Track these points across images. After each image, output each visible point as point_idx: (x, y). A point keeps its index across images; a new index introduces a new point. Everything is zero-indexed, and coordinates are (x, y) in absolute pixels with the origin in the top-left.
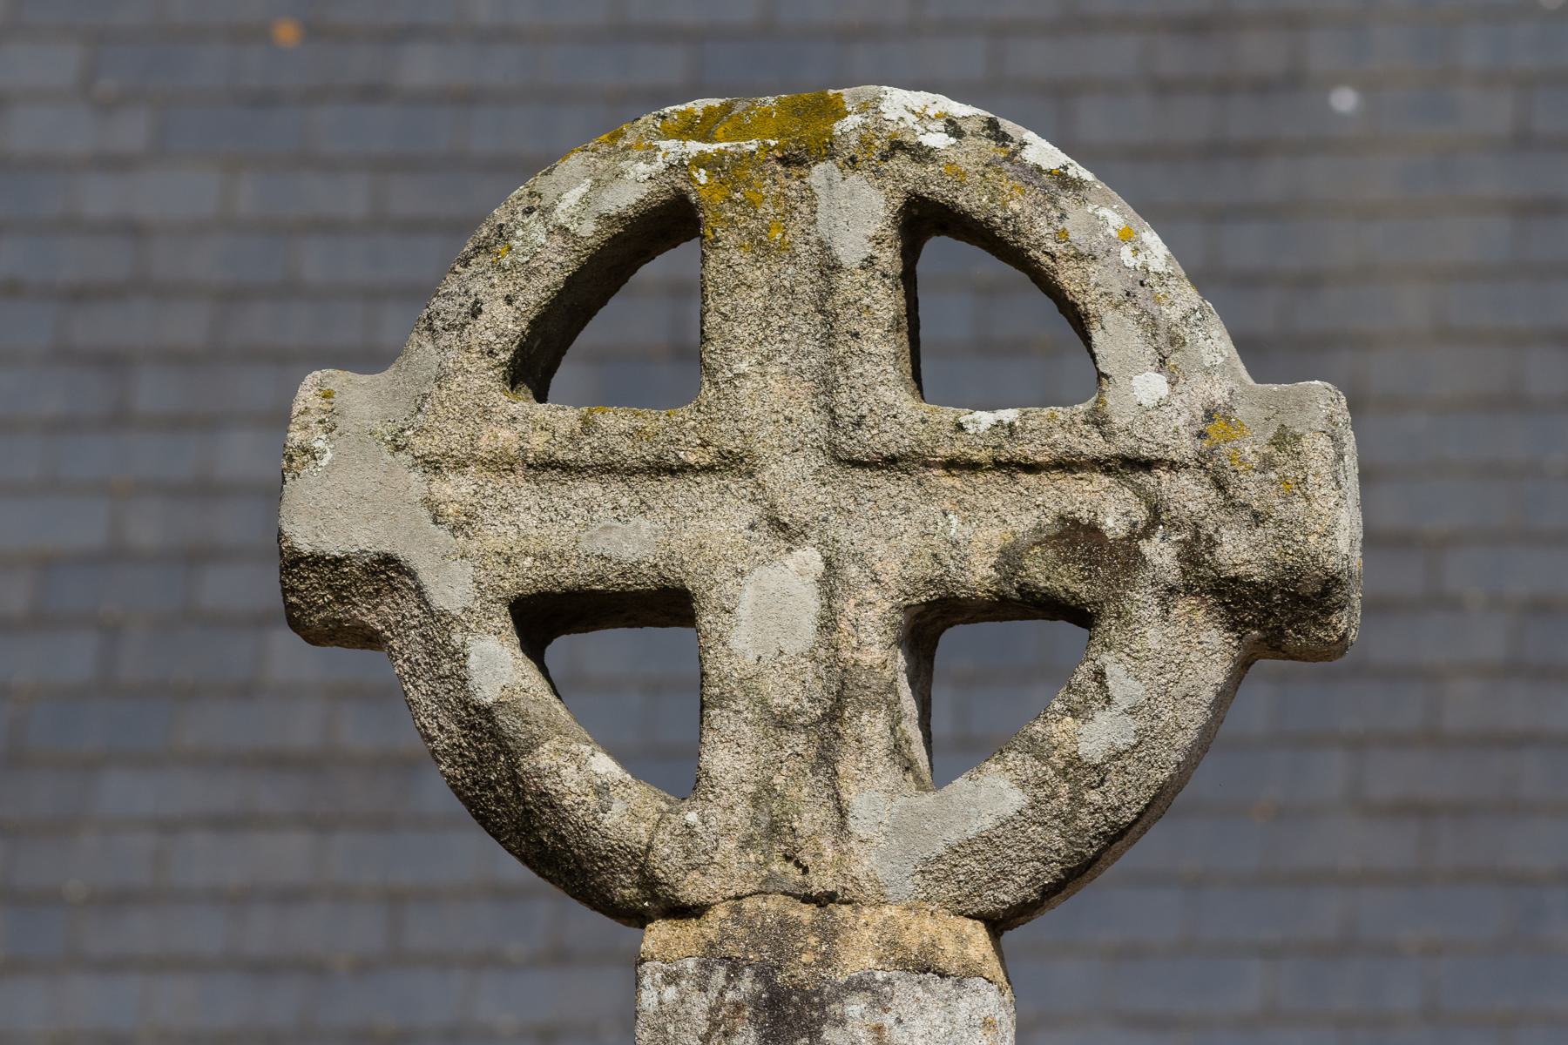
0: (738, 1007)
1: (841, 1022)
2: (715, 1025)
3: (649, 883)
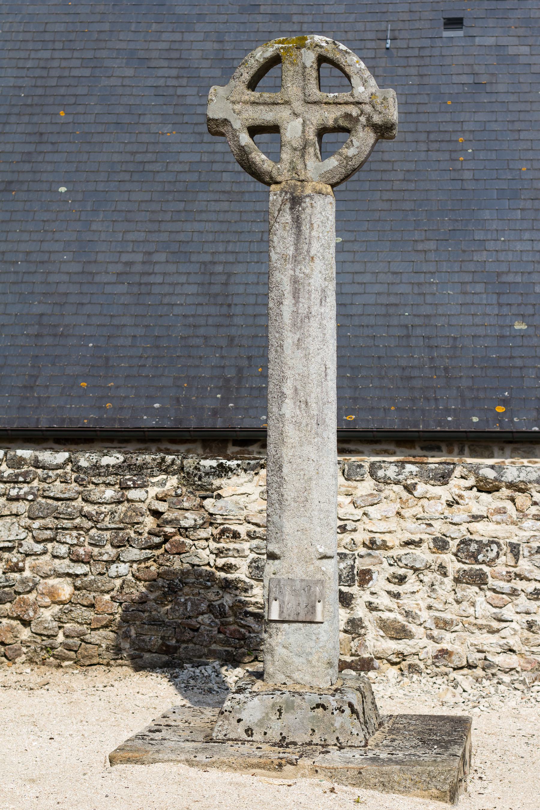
0: (287, 200)
1: (305, 202)
3: (271, 178)
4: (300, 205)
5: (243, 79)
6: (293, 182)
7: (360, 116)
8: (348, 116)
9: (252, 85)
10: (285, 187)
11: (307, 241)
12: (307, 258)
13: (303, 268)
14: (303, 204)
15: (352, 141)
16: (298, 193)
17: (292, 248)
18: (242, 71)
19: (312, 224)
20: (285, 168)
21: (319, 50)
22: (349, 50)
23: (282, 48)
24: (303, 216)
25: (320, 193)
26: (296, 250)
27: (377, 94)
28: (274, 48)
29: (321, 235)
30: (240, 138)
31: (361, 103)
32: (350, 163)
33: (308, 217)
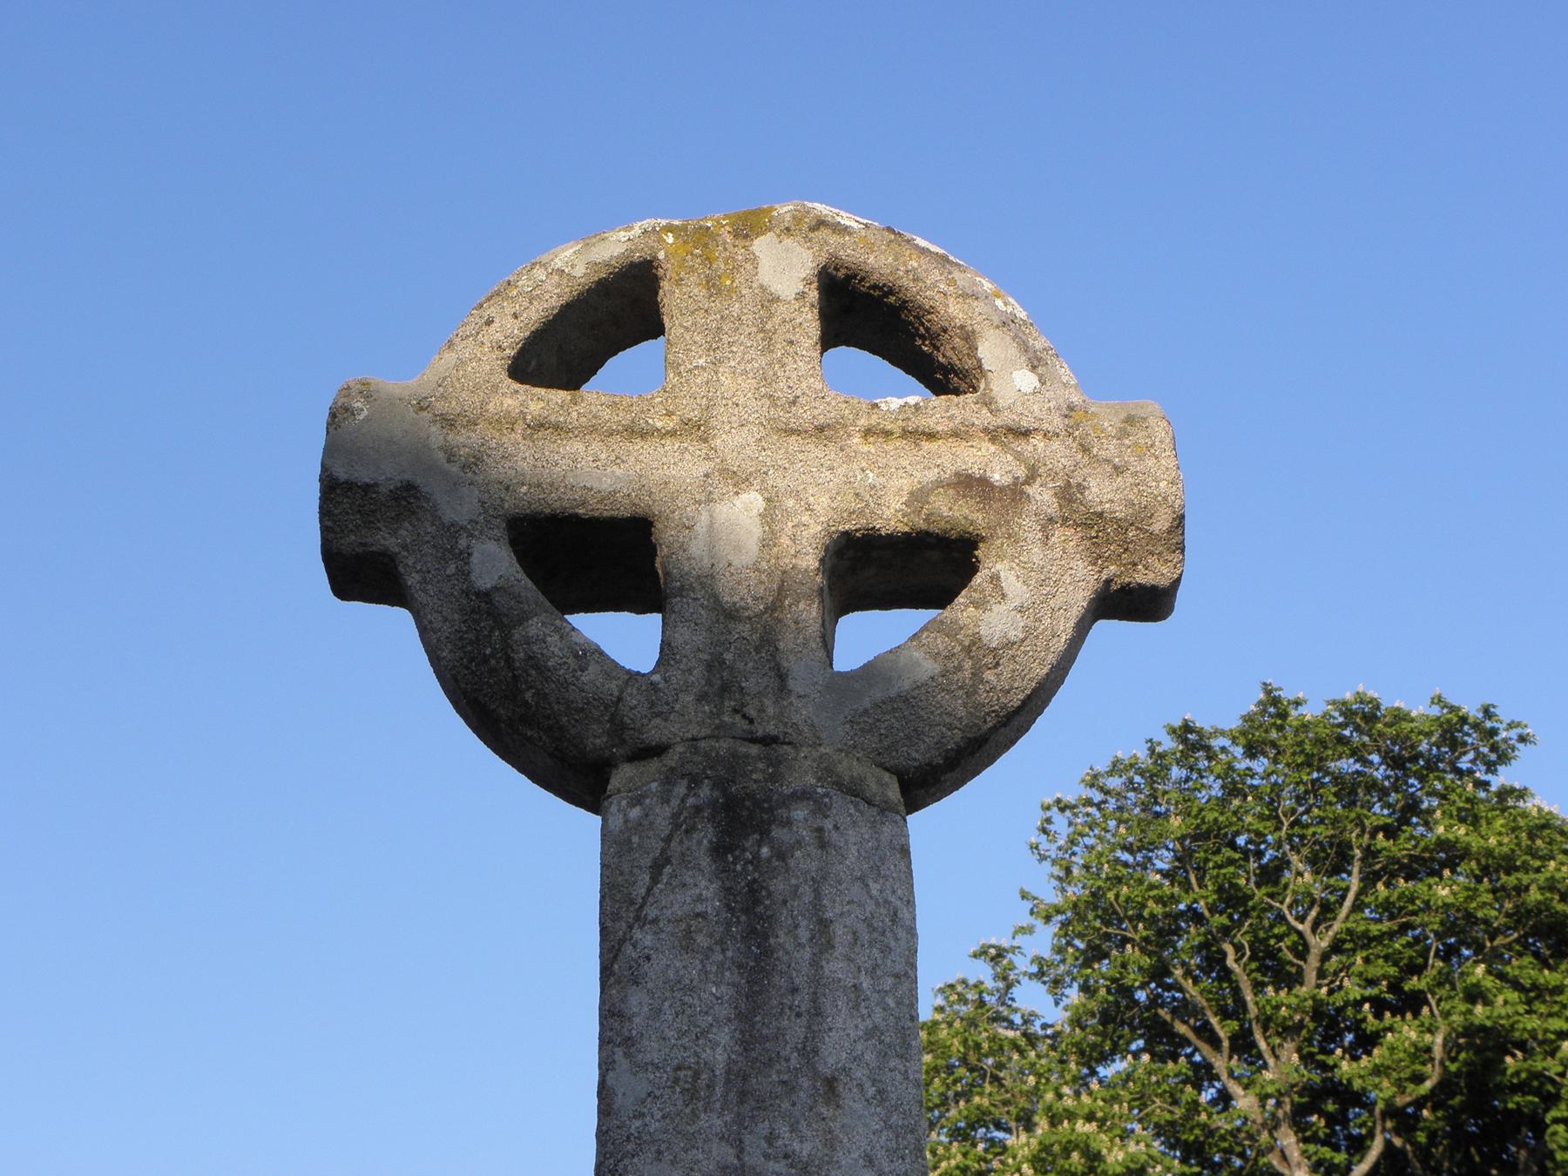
0: (698, 809)
1: (788, 823)
2: (677, 826)
3: (618, 728)
4: (765, 834)
5: (494, 333)
8: (971, 485)
11: (802, 1001)
12: (805, 1083)
13: (784, 1130)
14: (777, 833)
17: (724, 1036)
19: (824, 924)
20: (686, 688)
21: (834, 239)
23: (669, 228)
24: (778, 886)
25: (854, 791)
26: (747, 1042)
29: (866, 983)
30: (476, 558)
31: (1025, 434)
33: (806, 890)
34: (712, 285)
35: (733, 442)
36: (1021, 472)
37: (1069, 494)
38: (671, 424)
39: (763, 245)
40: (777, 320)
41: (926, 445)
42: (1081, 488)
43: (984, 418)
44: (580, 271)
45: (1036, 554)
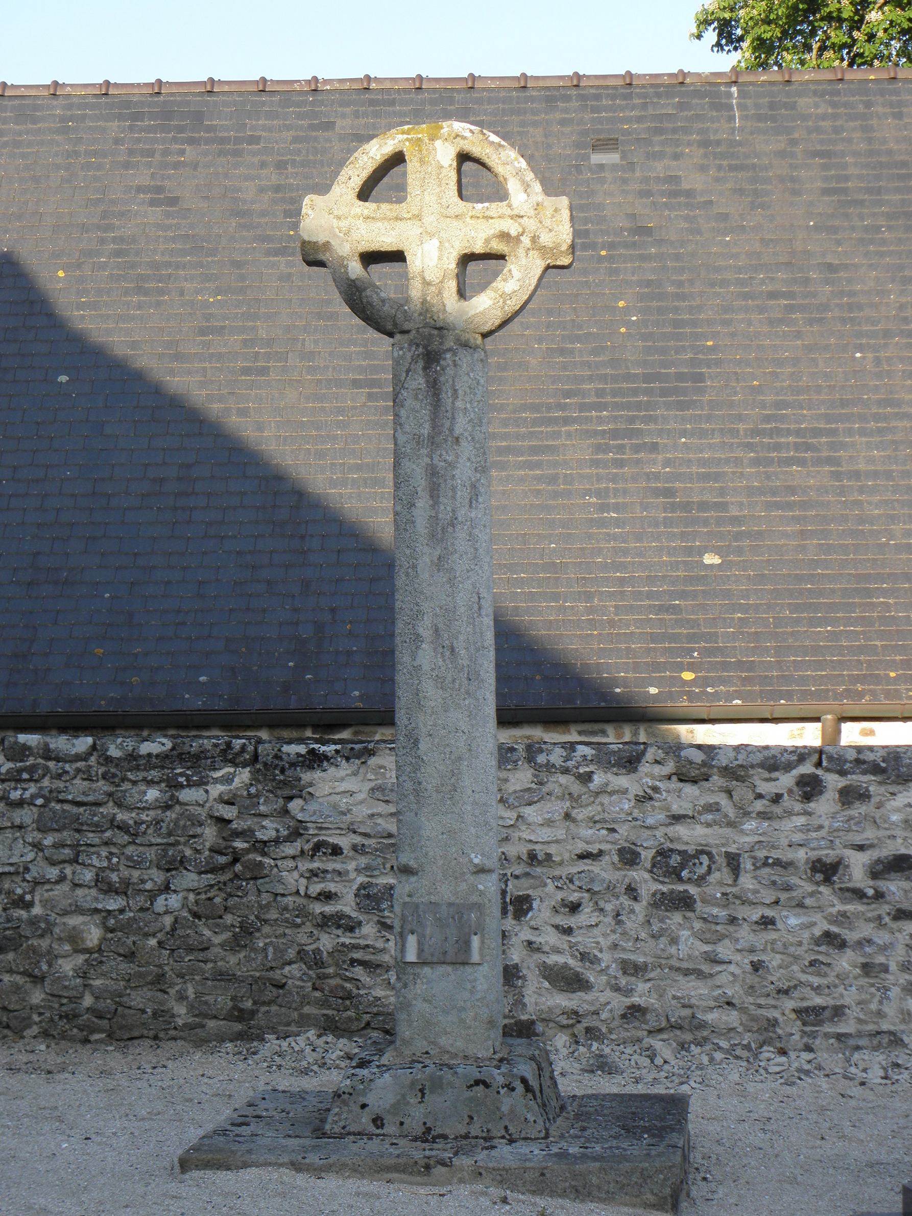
0: (419, 355)
1: (445, 359)
2: (413, 360)
3: (395, 324)
4: (438, 362)
6: (426, 330)
7: (522, 235)
8: (504, 236)
9: (364, 194)
10: (415, 338)
11: (449, 415)
12: (450, 439)
13: (444, 453)
14: (442, 362)
15: (510, 271)
16: (434, 346)
17: (427, 426)
18: (350, 172)
19: (456, 391)
21: (462, 142)
22: (503, 143)
23: (407, 139)
24: (442, 379)
26: (434, 426)
27: (545, 204)
28: (396, 141)
29: (468, 406)
32: (508, 302)
33: (450, 380)
34: (422, 161)
35: (429, 220)
36: (520, 230)
37: (534, 239)
38: (409, 216)
39: (438, 143)
40: (442, 175)
41: (490, 221)
42: (539, 237)
43: (509, 212)
44: (378, 157)
45: (524, 261)
